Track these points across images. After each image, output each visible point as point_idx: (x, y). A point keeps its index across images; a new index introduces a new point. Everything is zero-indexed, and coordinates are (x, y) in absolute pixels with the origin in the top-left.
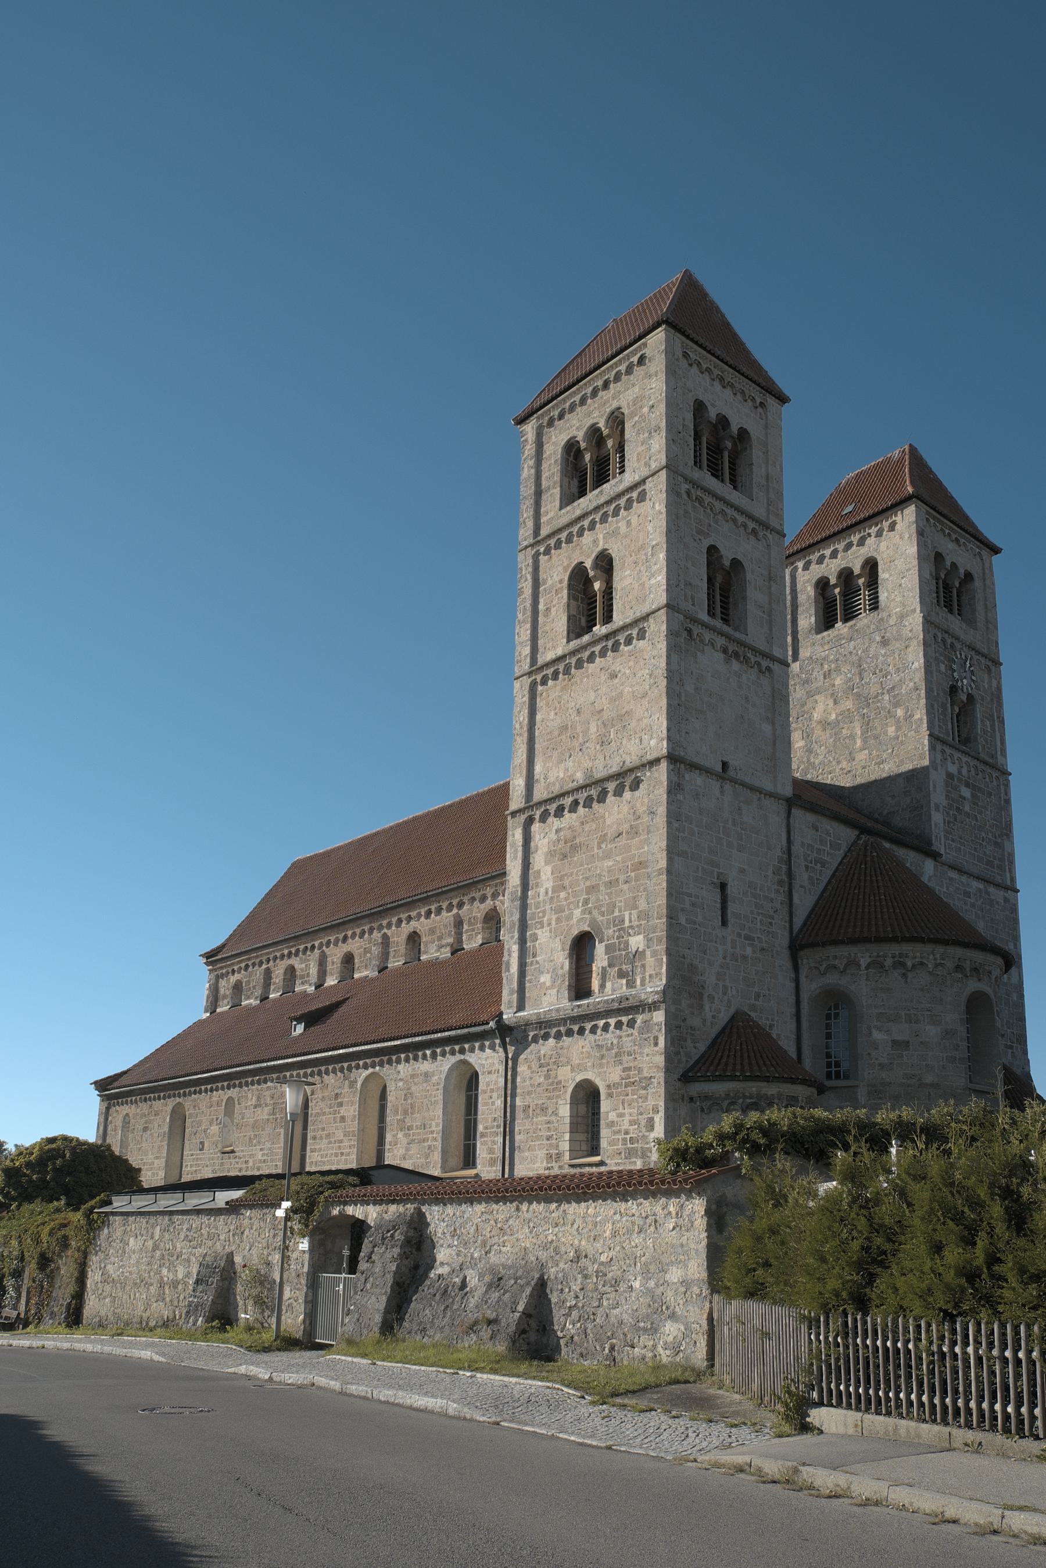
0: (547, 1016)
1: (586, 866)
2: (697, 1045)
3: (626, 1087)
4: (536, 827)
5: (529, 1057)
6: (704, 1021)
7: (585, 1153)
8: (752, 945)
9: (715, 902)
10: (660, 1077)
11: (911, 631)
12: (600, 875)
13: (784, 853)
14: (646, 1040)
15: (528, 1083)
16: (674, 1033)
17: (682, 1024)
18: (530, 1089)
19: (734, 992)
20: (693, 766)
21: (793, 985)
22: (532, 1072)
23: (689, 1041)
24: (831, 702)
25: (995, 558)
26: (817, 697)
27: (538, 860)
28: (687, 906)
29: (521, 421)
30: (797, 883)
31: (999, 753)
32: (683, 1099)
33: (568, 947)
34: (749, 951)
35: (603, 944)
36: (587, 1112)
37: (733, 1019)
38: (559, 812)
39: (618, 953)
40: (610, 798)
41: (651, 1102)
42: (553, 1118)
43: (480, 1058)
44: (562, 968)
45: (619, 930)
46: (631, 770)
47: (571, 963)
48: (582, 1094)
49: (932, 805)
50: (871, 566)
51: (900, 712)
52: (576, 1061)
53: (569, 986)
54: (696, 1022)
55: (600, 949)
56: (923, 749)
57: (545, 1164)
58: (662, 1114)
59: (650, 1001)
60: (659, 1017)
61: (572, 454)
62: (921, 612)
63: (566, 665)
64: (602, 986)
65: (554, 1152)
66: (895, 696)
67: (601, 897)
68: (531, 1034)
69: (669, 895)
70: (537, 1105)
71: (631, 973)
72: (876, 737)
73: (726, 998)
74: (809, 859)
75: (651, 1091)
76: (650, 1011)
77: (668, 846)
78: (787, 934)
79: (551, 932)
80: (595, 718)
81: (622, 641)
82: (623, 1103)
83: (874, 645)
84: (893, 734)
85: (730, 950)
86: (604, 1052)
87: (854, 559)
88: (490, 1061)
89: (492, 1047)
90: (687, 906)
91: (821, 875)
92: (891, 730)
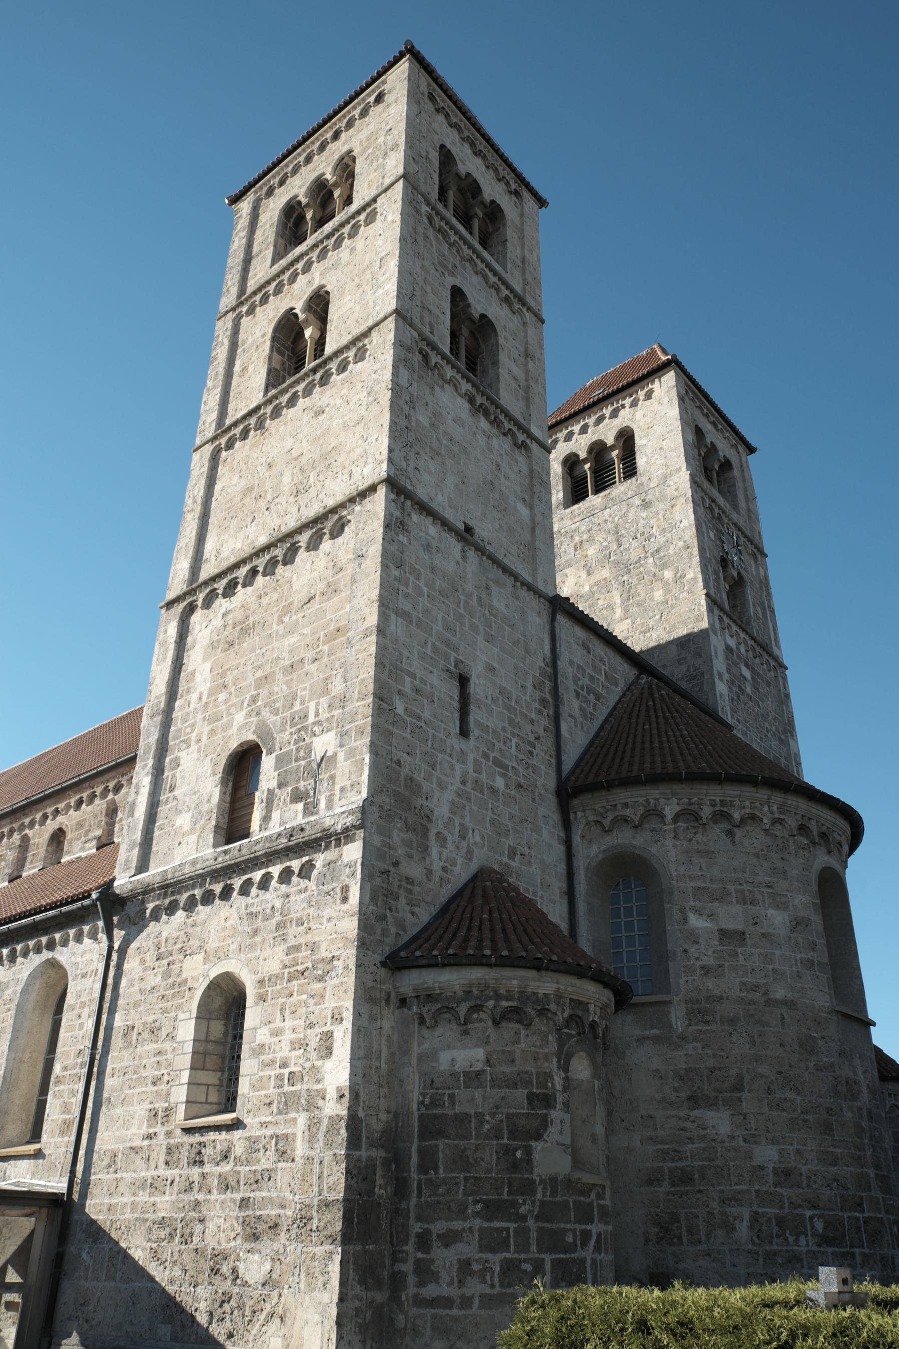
0: (177, 874)
1: (258, 651)
2: (416, 910)
3: (289, 981)
4: (197, 618)
5: (144, 944)
7: (215, 1107)
8: (503, 775)
10: (349, 955)
11: (676, 490)
12: (277, 659)
13: (547, 665)
14: (328, 893)
15: (136, 988)
16: (378, 881)
17: (392, 869)
18: (139, 997)
19: (478, 839)
20: (424, 509)
21: (562, 848)
22: (145, 970)
23: (403, 900)
24: (583, 574)
25: (751, 458)
26: (567, 571)
27: (195, 659)
28: (407, 689)
29: (236, 199)
30: (565, 710)
31: (773, 643)
32: (388, 1001)
33: (221, 769)
34: (500, 783)
35: (274, 755)
36: (226, 1034)
37: (474, 878)
38: (230, 590)
39: (294, 764)
40: (302, 555)
41: (330, 1003)
42: (167, 1046)
43: (73, 954)
44: (209, 801)
45: (299, 730)
46: (333, 511)
47: (223, 793)
48: (218, 1002)
49: (715, 672)
50: (626, 438)
51: (668, 574)
52: (213, 944)
53: (217, 826)
54: (415, 871)
55: (267, 763)
56: (699, 610)
57: (144, 1130)
58: (348, 1023)
59: (339, 828)
60: (353, 852)
61: (292, 220)
62: (687, 470)
63: (259, 418)
64: (266, 819)
65: (161, 1105)
66: (661, 558)
67: (276, 689)
68: (150, 906)
69: (380, 664)
70: (145, 1024)
71: (312, 792)
72: (639, 605)
73: (464, 844)
74: (580, 683)
75: (331, 982)
76: (338, 844)
77: (381, 595)
78: (552, 773)
79: (199, 751)
80: (290, 466)
81: (334, 370)
82: (282, 1011)
83: (633, 510)
84: (661, 598)
86: (259, 923)
87: (607, 432)
88: (87, 956)
89: (93, 936)
90: (407, 689)
91: (595, 709)
92: (658, 595)
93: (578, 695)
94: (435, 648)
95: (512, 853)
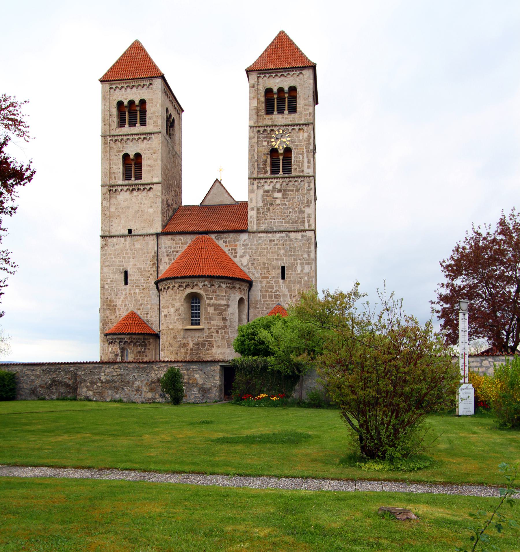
6: (116, 317)
9: (122, 278)
19: (130, 305)
23: (110, 323)
34: (137, 291)
54: (113, 317)
73: (126, 308)
85: (128, 292)
93: (168, 256)
94: (116, 269)
95: (141, 305)
